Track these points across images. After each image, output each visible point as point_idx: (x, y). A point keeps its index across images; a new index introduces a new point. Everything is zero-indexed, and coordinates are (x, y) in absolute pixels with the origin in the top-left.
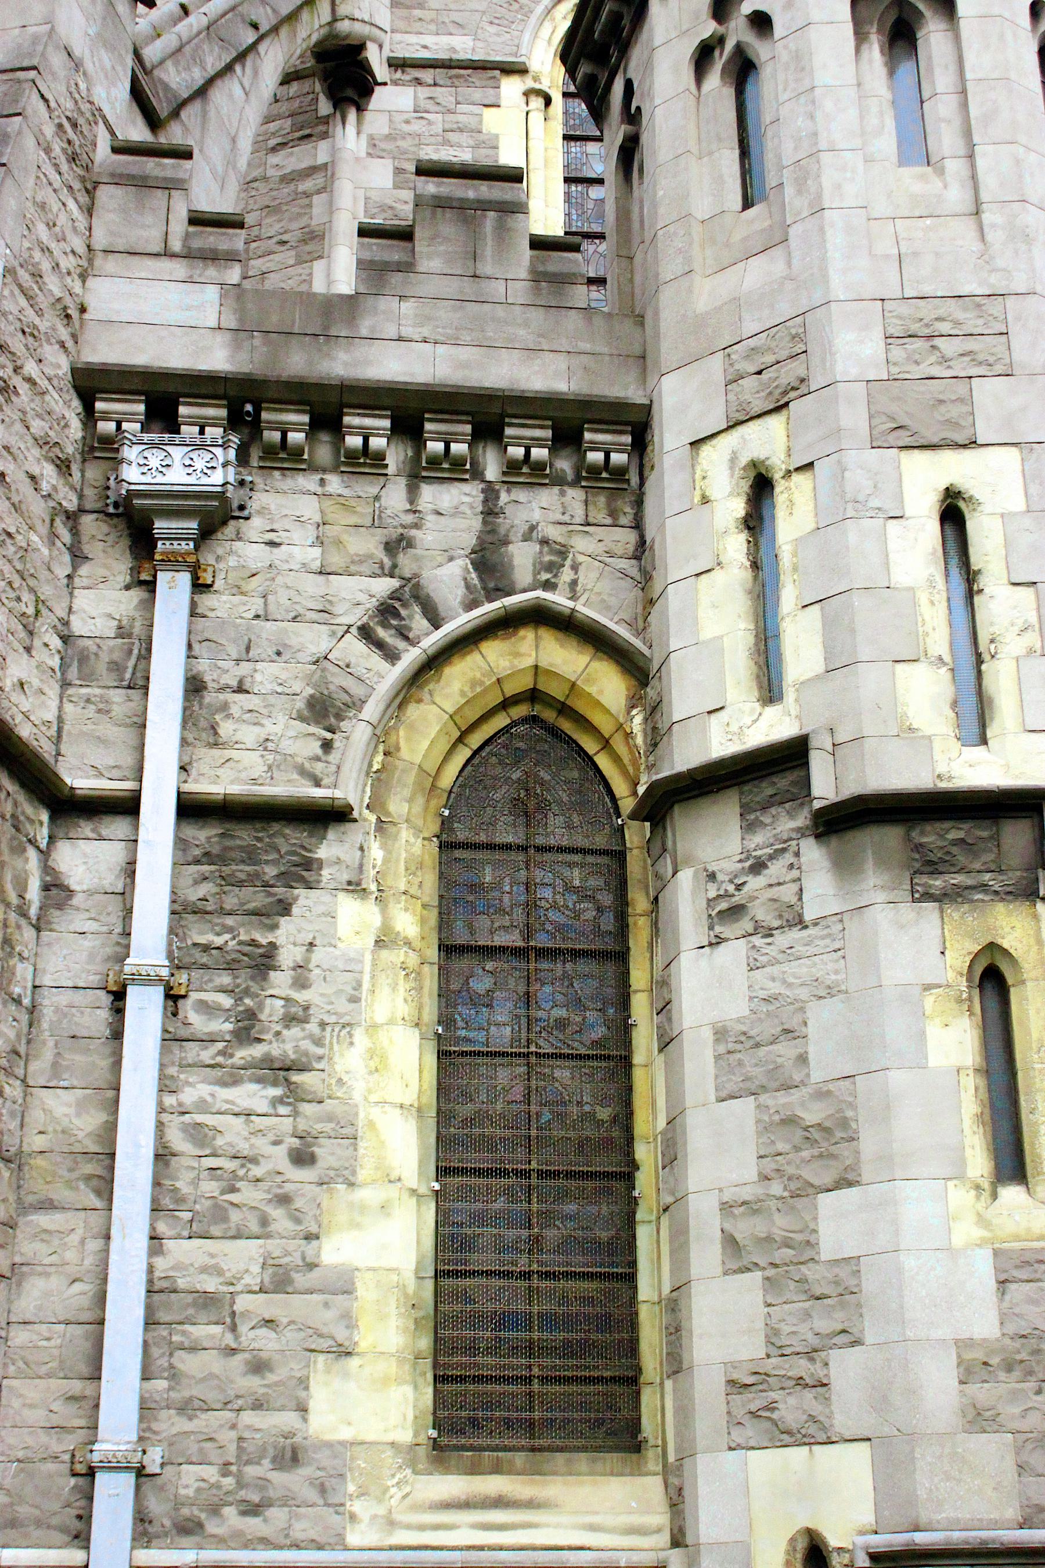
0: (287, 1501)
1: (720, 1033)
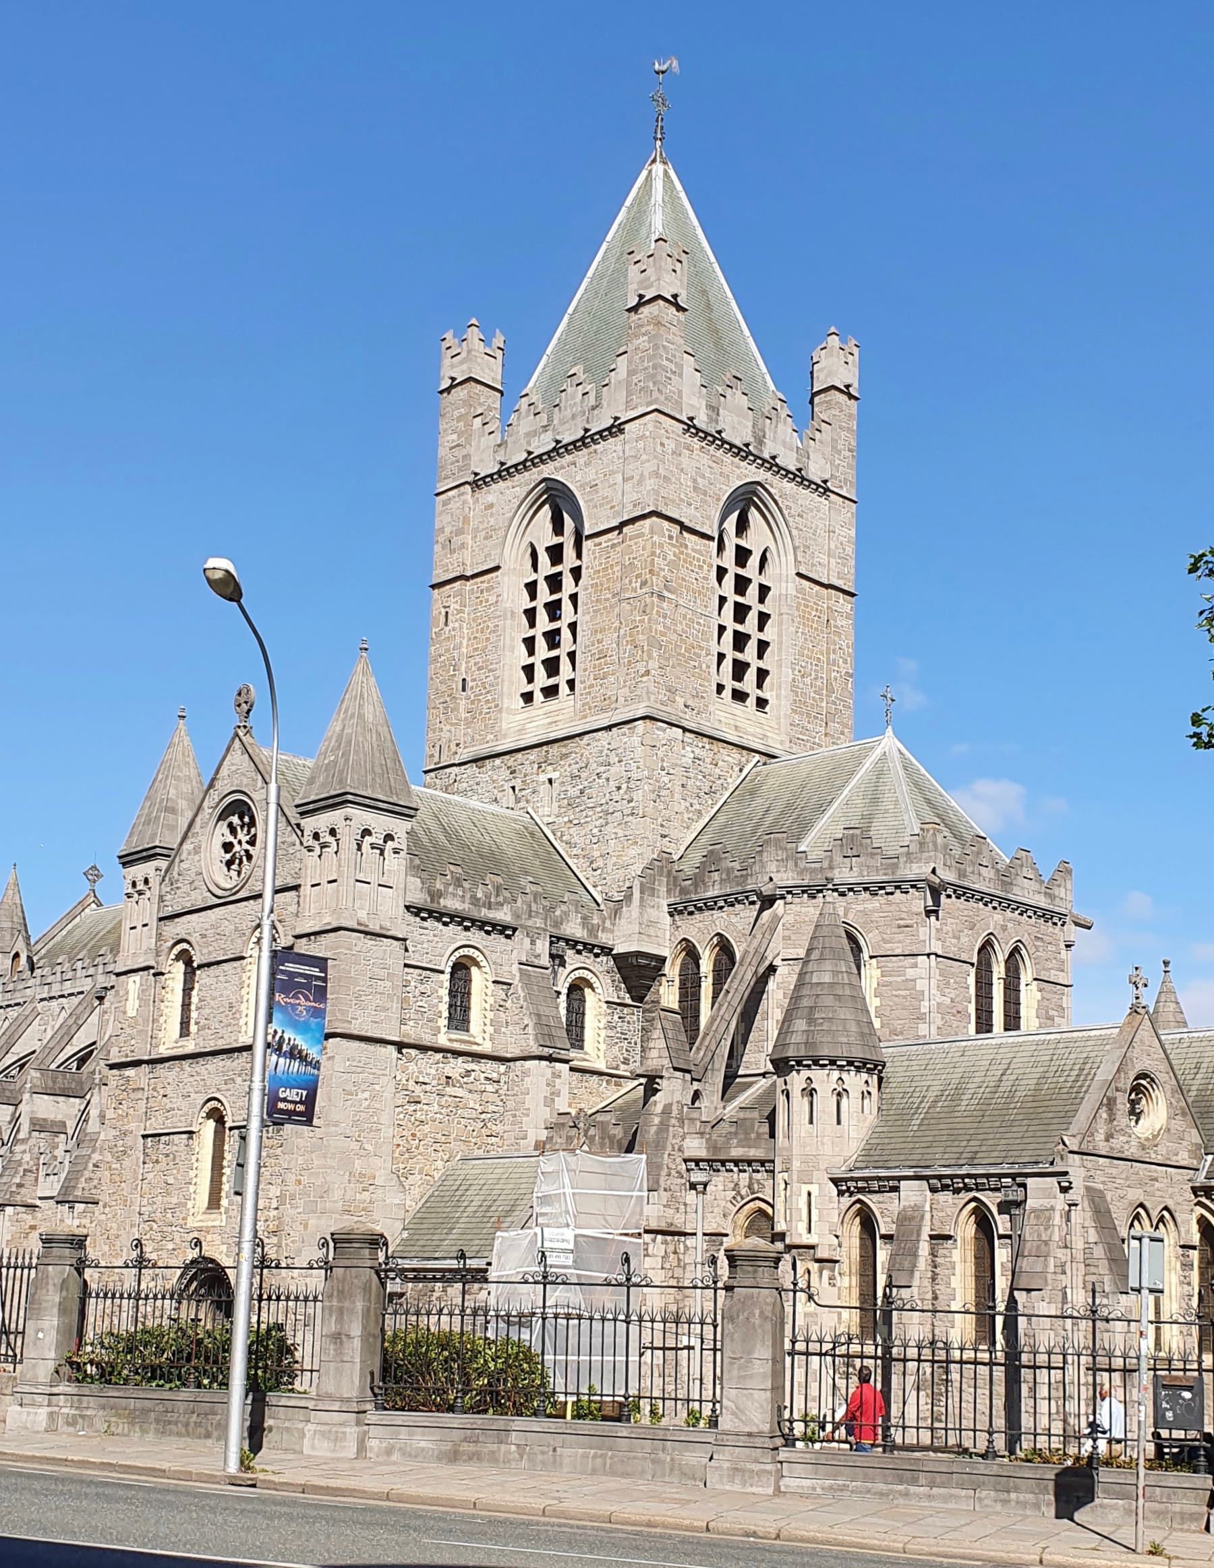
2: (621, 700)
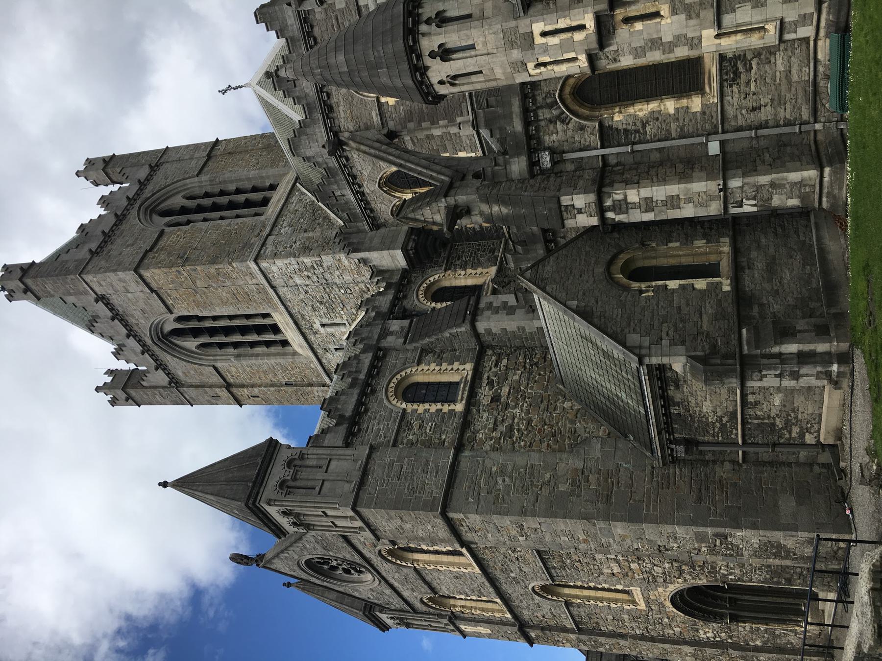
0: (710, 113)
1: (635, 58)
2: (254, 281)
